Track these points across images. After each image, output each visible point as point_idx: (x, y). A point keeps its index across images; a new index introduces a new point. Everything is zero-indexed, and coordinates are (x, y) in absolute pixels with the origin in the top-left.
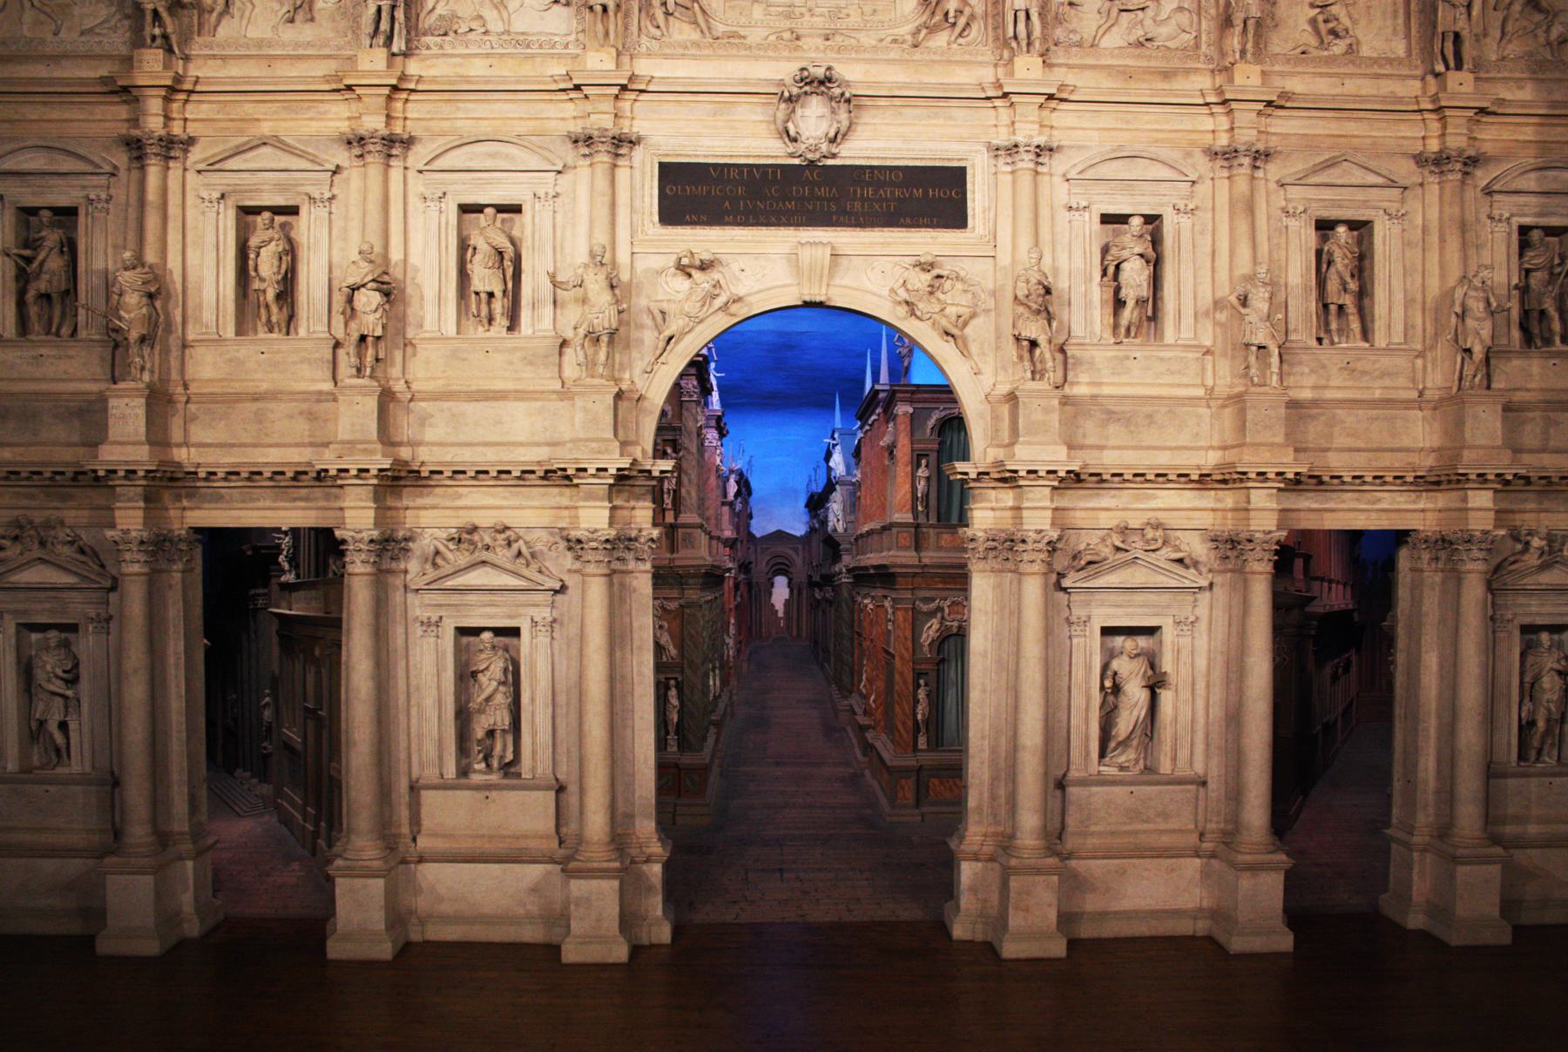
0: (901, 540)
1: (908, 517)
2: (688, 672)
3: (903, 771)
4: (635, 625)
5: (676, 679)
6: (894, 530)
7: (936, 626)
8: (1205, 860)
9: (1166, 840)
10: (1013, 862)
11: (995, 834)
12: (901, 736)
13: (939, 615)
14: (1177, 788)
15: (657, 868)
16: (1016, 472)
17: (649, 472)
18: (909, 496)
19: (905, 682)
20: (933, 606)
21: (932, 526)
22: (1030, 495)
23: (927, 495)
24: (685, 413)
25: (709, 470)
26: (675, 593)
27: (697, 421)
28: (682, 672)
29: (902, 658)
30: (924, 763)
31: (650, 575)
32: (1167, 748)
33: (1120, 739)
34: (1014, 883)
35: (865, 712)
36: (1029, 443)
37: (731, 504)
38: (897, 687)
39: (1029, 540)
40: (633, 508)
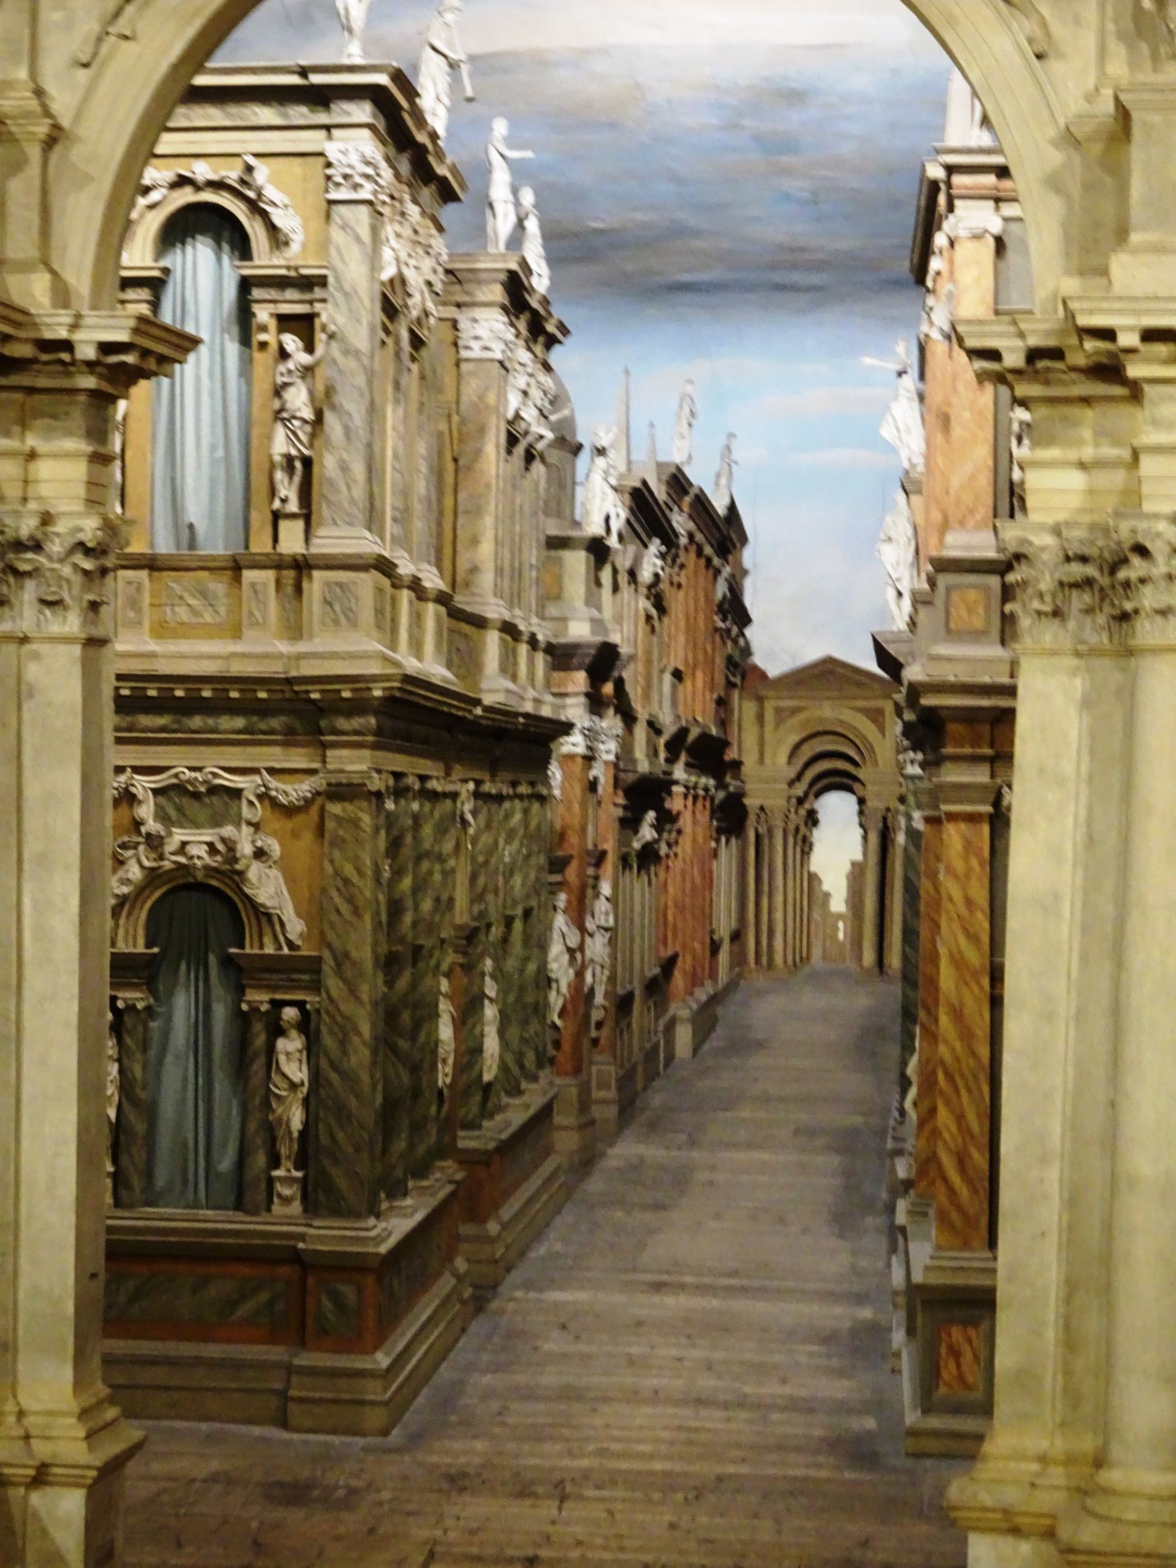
0: (959, 612)
2: (333, 983)
4: (32, 790)
5: (300, 1005)
11: (1070, 1460)
12: (951, 1191)
16: (1108, 334)
17: (67, 345)
18: (984, 480)
19: (966, 1035)
22: (1169, 411)
24: (337, 235)
25: (482, 430)
26: (298, 759)
27: (374, 261)
28: (316, 986)
29: (958, 962)
31: (77, 650)
36: (1158, 249)
37: (598, 550)
39: (1158, 548)
40: (32, 456)
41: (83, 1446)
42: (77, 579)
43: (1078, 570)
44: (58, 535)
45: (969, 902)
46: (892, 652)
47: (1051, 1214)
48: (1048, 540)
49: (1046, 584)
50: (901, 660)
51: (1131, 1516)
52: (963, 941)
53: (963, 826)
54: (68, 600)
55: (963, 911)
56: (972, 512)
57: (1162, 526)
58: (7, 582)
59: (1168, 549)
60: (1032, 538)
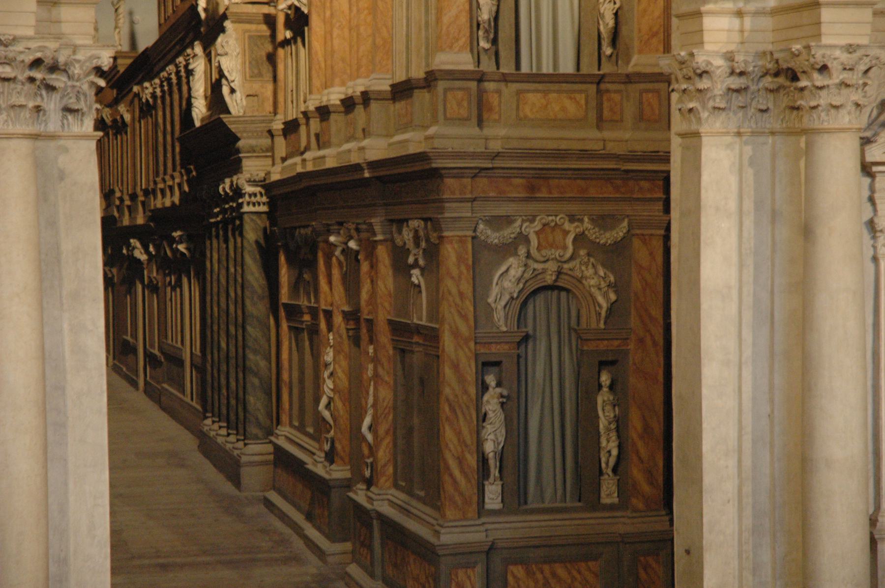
1: (464, 61)
4: (66, 246)
6: (441, 85)
7: (515, 272)
12: (455, 481)
13: (522, 251)
18: (464, 19)
19: (461, 379)
20: (509, 233)
21: (505, 79)
23: (496, 19)
29: (456, 334)
30: (499, 535)
35: (331, 457)
38: (447, 391)
39: (833, 65)
42: (91, 93)
43: (736, 82)
44: (78, 61)
45: (461, 294)
46: (233, 131)
47: (730, 487)
48: (719, 62)
49: (719, 89)
50: (239, 135)
52: (457, 318)
53: (456, 246)
54: (85, 109)
55: (458, 300)
56: (457, 40)
57: (837, 53)
58: (41, 95)
59: (840, 67)
60: (712, 61)
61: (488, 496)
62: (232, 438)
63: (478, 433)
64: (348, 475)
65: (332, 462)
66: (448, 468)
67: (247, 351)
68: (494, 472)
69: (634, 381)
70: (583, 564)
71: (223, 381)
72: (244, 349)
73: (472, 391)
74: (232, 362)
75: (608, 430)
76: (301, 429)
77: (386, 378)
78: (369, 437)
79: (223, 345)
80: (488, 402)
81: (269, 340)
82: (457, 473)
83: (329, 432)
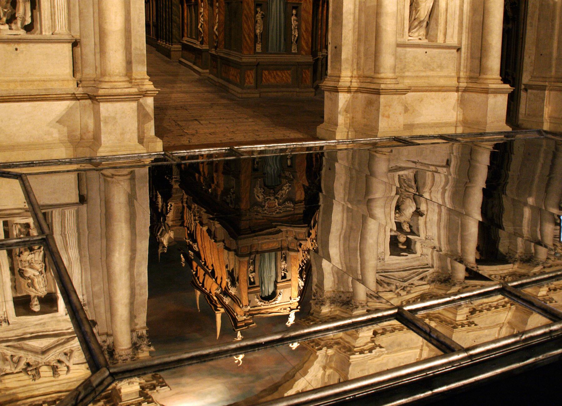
3: (249, 66)
8: (460, 93)
9: (442, 82)
10: (383, 86)
12: (247, 42)
14: (447, 51)
15: (150, 102)
30: (260, 60)
32: (441, 27)
33: (422, 19)
34: (383, 99)
35: (202, 43)
38: (245, 12)
41: (153, 86)
47: (351, 25)
51: (389, 83)
61: (257, 48)
62: (168, 44)
63: (255, 27)
64: (208, 48)
65: (202, 44)
66: (245, 37)
67: (173, 15)
68: (259, 40)
69: (303, 13)
70: (286, 71)
71: (164, 27)
72: (171, 14)
73: (253, 12)
74: (167, 20)
75: (295, 28)
76: (191, 38)
77: (222, 13)
78: (217, 33)
79: (164, 15)
80: (258, 17)
81: (179, 12)
82: (247, 39)
83: (201, 35)
